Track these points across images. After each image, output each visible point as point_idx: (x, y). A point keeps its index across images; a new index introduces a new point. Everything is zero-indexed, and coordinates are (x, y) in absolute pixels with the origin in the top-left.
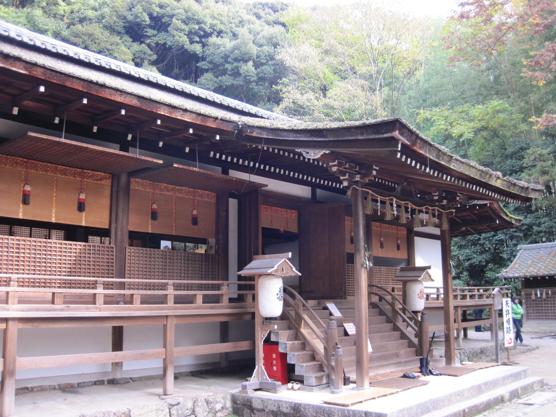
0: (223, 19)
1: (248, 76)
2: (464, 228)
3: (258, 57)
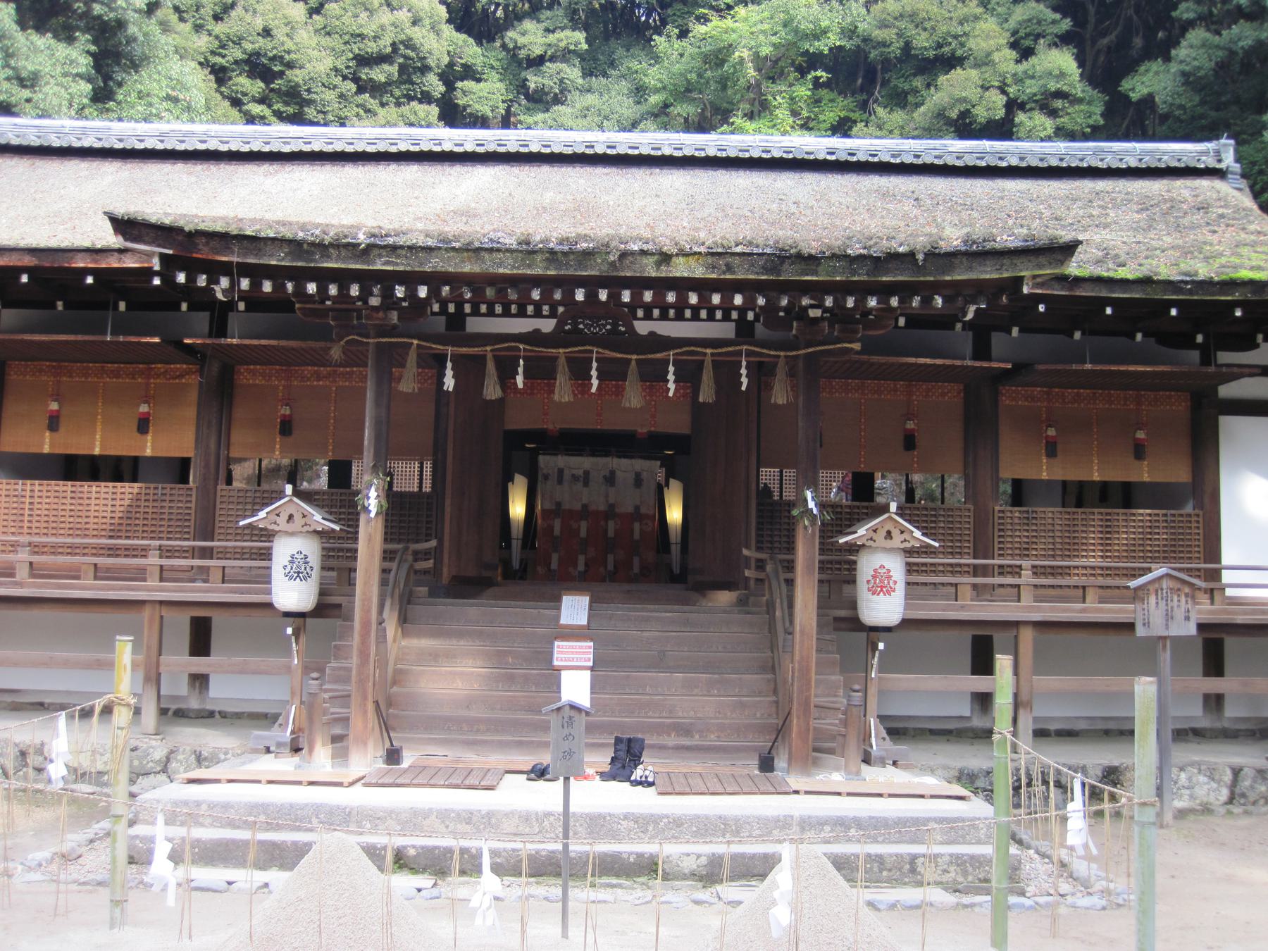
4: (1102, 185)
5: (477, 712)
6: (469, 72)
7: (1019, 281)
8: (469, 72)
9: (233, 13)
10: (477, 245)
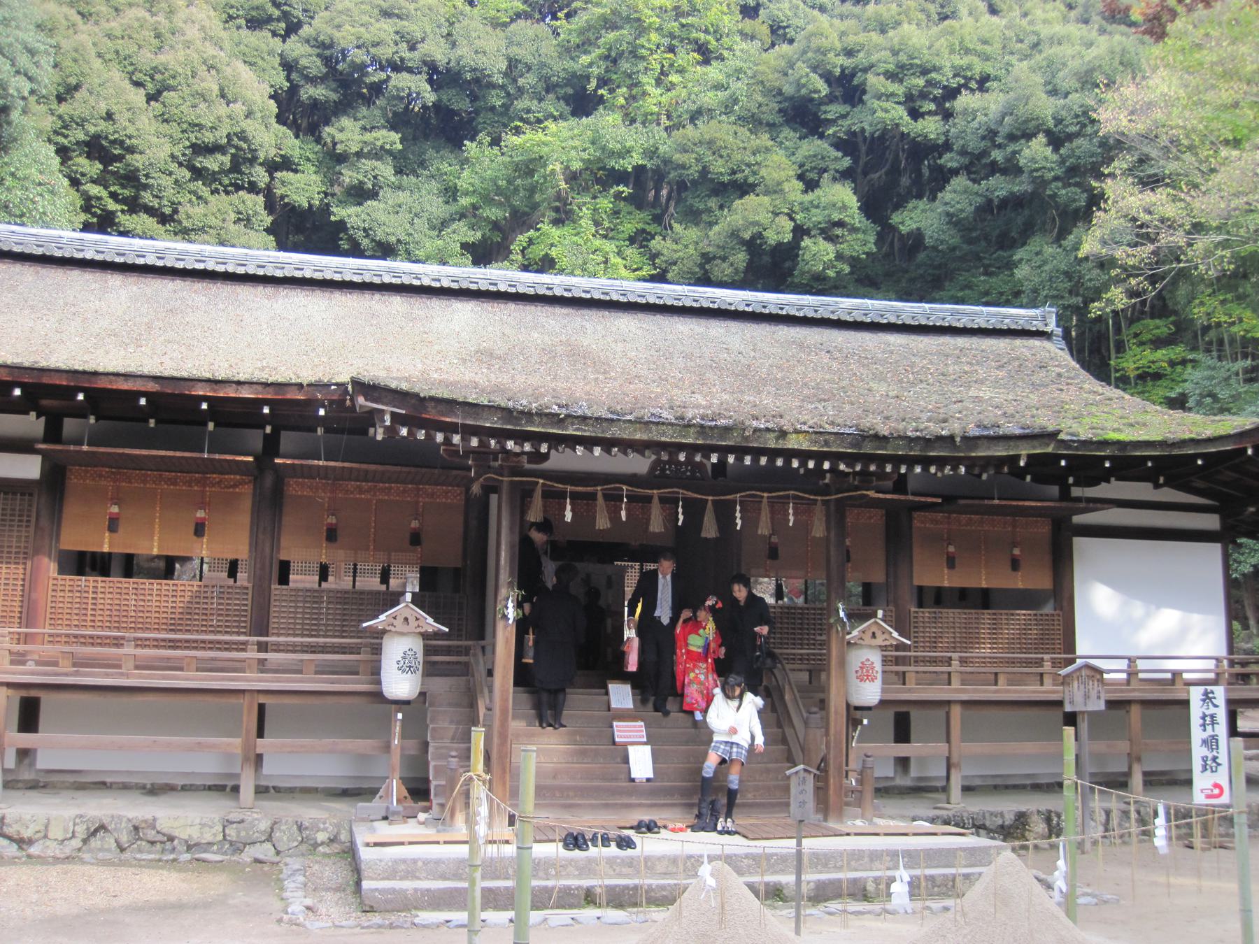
0: (988, 49)
1: (1036, 170)
2: (1252, 509)
3: (1059, 121)
4: (961, 341)
5: (565, 781)
6: (286, 164)
7: (1018, 457)
8: (286, 164)
9: (77, 95)
10: (646, 419)
